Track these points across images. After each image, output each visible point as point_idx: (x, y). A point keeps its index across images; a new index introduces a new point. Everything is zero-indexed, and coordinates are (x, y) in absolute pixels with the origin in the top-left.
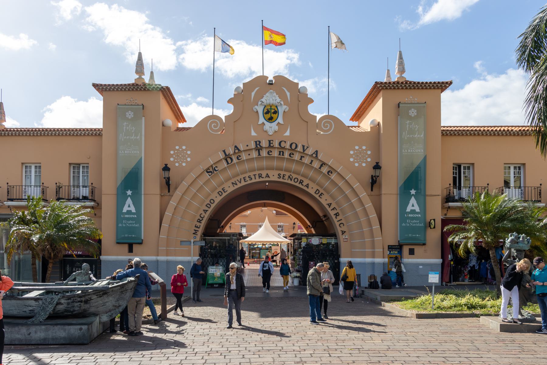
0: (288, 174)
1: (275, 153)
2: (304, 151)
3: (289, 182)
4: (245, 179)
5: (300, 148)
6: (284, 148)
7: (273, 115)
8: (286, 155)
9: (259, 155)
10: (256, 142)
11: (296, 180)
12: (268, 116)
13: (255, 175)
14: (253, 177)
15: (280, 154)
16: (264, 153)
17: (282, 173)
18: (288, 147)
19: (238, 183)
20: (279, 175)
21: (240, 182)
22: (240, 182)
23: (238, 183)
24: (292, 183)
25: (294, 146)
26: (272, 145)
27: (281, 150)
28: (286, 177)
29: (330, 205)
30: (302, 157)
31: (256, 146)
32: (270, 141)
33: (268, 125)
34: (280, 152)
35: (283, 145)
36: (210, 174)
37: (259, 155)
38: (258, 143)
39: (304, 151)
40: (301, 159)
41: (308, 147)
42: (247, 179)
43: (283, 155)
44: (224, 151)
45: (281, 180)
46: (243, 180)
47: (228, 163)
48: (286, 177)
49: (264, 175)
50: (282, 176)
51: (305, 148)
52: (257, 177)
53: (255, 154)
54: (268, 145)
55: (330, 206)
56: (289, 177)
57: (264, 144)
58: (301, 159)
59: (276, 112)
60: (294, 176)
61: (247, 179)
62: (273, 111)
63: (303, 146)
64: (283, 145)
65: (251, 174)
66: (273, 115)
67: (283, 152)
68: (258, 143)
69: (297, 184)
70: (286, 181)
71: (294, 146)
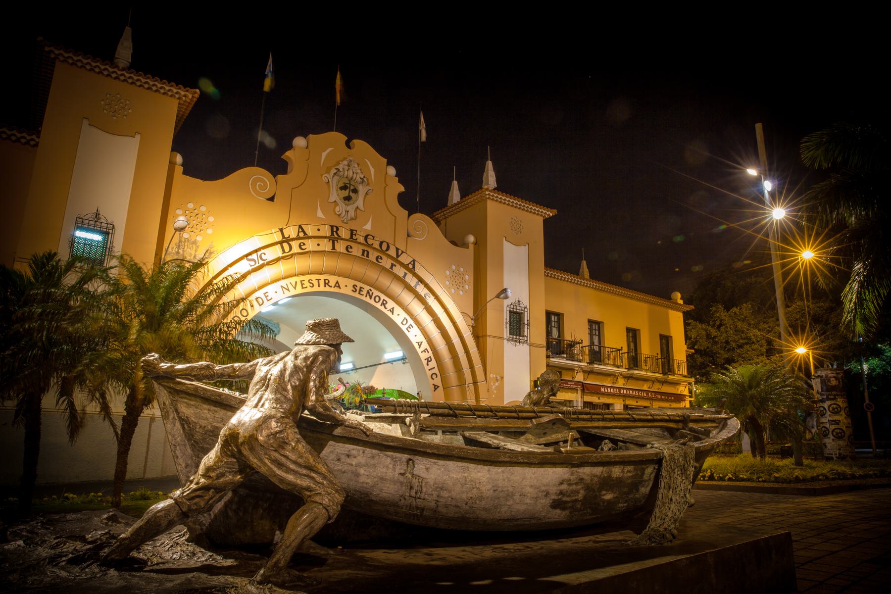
0: (367, 288)
1: (357, 251)
2: (398, 256)
3: (367, 299)
4: (302, 284)
5: (392, 252)
6: (370, 246)
7: (351, 194)
8: (373, 256)
9: (334, 248)
10: (332, 227)
11: (377, 299)
12: (346, 193)
13: (319, 280)
14: (315, 282)
15: (363, 254)
16: (341, 247)
17: (359, 284)
18: (376, 245)
19: (291, 288)
20: (354, 286)
21: (295, 288)
22: (295, 288)
23: (291, 288)
24: (372, 302)
25: (384, 247)
26: (354, 237)
27: (366, 249)
28: (364, 292)
29: (420, 344)
30: (392, 265)
31: (332, 234)
32: (352, 231)
33: (341, 208)
34: (364, 251)
35: (370, 241)
36: (252, 263)
37: (334, 248)
38: (335, 229)
39: (398, 256)
40: (391, 268)
41: (403, 252)
42: (307, 284)
43: (367, 256)
44: (281, 230)
45: (356, 295)
46: (299, 285)
47: (284, 252)
48: (364, 292)
49: (332, 283)
50: (358, 289)
51: (400, 252)
52: (322, 283)
53: (326, 246)
54: (348, 237)
55: (420, 346)
56: (368, 292)
57: (344, 233)
58: (391, 268)
59: (355, 191)
60: (376, 293)
61: (307, 284)
62: (352, 188)
63: (397, 249)
64: (370, 241)
65: (314, 278)
66: (351, 194)
67: (368, 252)
68: (335, 229)
69: (378, 305)
70: (363, 298)
71: (384, 247)
